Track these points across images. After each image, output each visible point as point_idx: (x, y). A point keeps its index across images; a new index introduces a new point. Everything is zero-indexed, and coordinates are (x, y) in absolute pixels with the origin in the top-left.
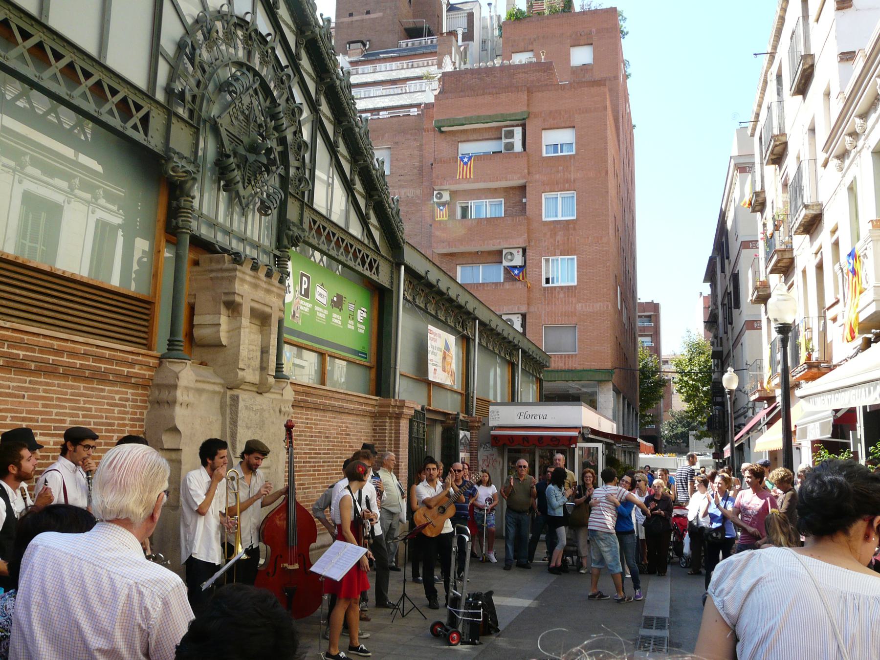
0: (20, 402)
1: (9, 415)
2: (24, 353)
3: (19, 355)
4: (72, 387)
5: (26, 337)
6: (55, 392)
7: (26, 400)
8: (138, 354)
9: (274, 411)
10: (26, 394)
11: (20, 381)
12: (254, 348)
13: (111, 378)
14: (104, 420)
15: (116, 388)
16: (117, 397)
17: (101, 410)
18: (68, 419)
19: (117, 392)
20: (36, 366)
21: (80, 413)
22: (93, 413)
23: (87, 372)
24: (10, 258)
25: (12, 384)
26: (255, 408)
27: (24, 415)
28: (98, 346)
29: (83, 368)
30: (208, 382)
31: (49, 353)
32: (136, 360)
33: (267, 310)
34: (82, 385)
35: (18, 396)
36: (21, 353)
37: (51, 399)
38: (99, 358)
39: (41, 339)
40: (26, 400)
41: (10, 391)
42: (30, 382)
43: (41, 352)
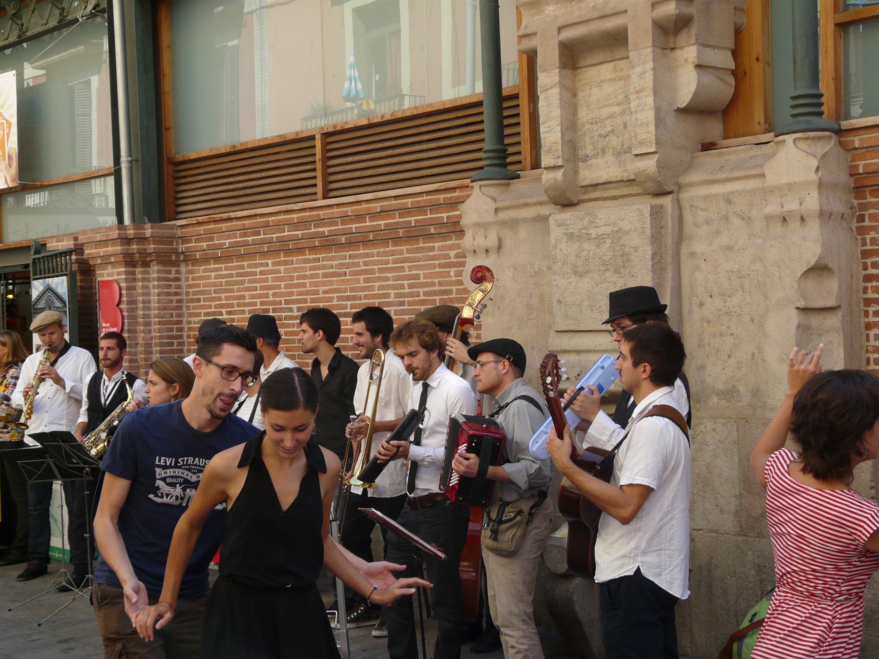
0: (343, 280)
1: (335, 295)
2: (328, 229)
3: (324, 232)
4: (393, 253)
5: (321, 213)
6: (375, 263)
7: (348, 277)
8: (454, 189)
9: (747, 220)
10: (347, 270)
11: (341, 258)
12: (617, 109)
13: (432, 231)
14: (437, 288)
15: (450, 242)
16: (452, 253)
17: (431, 275)
18: (393, 292)
19: (451, 248)
20: (346, 239)
21: (406, 282)
22: (422, 280)
23: (401, 231)
24: (330, 130)
25: (334, 263)
26: (594, 232)
27: (348, 294)
28: (396, 197)
29: (390, 228)
30: (526, 205)
31: (352, 222)
32: (451, 198)
33: (611, 24)
34: (404, 248)
35: (340, 275)
36: (326, 229)
37: (372, 272)
38: (405, 211)
39: (336, 210)
40: (348, 277)
41: (334, 270)
42: (350, 257)
43: (343, 223)
